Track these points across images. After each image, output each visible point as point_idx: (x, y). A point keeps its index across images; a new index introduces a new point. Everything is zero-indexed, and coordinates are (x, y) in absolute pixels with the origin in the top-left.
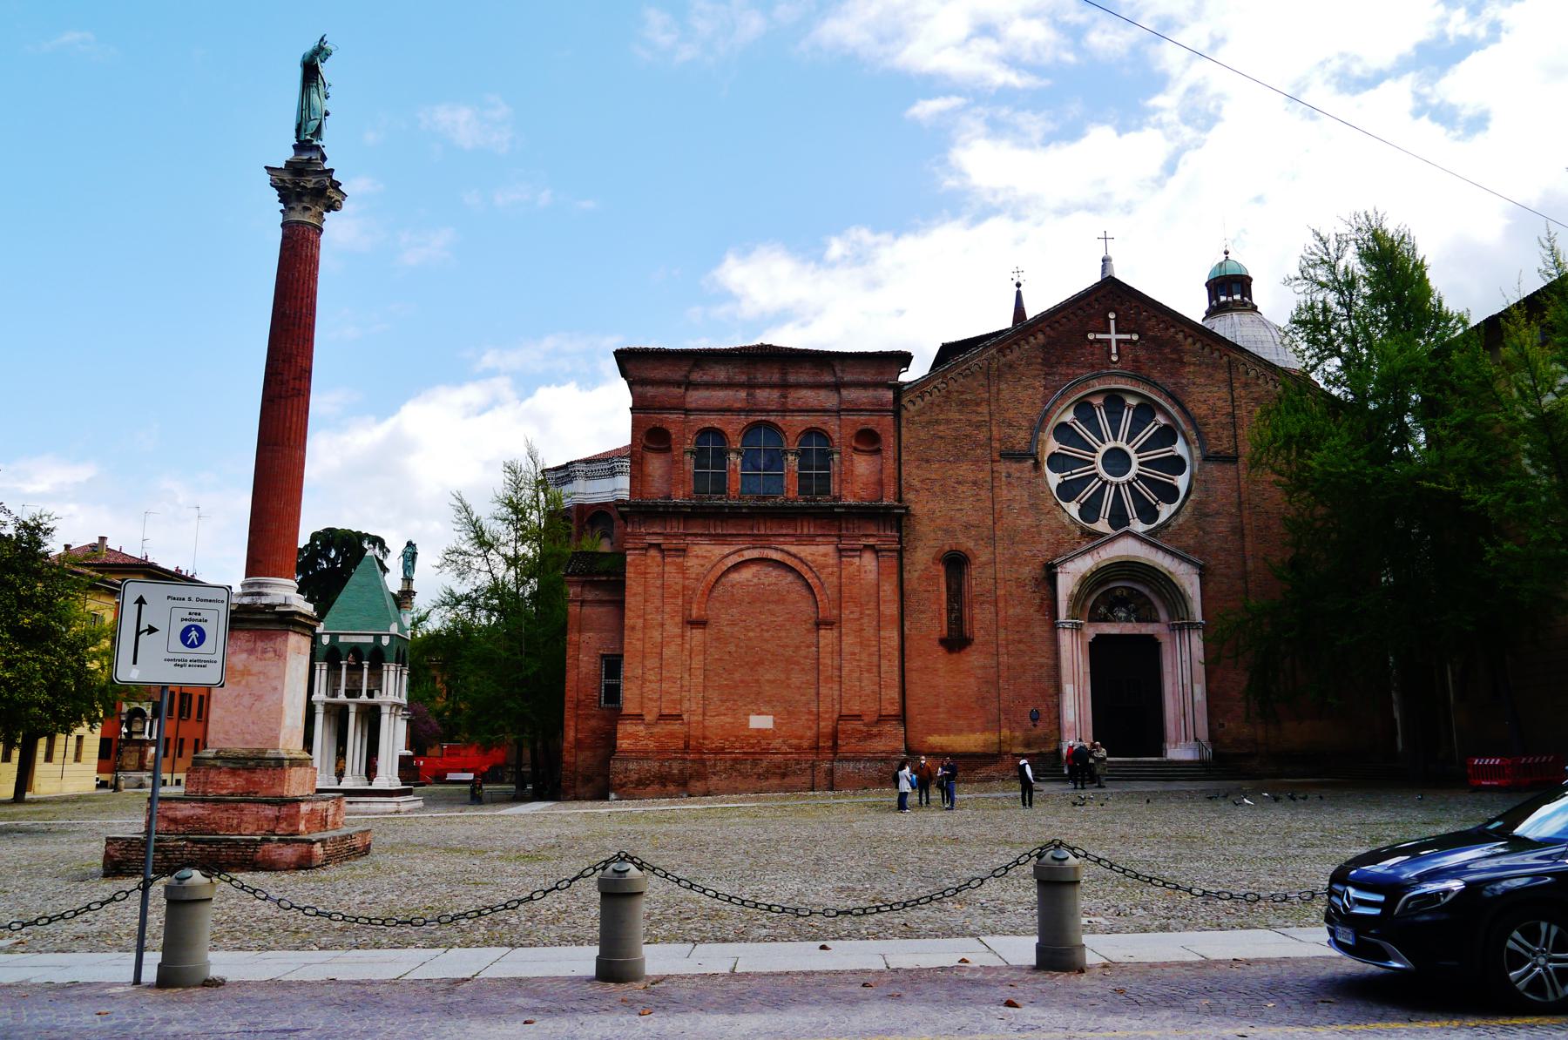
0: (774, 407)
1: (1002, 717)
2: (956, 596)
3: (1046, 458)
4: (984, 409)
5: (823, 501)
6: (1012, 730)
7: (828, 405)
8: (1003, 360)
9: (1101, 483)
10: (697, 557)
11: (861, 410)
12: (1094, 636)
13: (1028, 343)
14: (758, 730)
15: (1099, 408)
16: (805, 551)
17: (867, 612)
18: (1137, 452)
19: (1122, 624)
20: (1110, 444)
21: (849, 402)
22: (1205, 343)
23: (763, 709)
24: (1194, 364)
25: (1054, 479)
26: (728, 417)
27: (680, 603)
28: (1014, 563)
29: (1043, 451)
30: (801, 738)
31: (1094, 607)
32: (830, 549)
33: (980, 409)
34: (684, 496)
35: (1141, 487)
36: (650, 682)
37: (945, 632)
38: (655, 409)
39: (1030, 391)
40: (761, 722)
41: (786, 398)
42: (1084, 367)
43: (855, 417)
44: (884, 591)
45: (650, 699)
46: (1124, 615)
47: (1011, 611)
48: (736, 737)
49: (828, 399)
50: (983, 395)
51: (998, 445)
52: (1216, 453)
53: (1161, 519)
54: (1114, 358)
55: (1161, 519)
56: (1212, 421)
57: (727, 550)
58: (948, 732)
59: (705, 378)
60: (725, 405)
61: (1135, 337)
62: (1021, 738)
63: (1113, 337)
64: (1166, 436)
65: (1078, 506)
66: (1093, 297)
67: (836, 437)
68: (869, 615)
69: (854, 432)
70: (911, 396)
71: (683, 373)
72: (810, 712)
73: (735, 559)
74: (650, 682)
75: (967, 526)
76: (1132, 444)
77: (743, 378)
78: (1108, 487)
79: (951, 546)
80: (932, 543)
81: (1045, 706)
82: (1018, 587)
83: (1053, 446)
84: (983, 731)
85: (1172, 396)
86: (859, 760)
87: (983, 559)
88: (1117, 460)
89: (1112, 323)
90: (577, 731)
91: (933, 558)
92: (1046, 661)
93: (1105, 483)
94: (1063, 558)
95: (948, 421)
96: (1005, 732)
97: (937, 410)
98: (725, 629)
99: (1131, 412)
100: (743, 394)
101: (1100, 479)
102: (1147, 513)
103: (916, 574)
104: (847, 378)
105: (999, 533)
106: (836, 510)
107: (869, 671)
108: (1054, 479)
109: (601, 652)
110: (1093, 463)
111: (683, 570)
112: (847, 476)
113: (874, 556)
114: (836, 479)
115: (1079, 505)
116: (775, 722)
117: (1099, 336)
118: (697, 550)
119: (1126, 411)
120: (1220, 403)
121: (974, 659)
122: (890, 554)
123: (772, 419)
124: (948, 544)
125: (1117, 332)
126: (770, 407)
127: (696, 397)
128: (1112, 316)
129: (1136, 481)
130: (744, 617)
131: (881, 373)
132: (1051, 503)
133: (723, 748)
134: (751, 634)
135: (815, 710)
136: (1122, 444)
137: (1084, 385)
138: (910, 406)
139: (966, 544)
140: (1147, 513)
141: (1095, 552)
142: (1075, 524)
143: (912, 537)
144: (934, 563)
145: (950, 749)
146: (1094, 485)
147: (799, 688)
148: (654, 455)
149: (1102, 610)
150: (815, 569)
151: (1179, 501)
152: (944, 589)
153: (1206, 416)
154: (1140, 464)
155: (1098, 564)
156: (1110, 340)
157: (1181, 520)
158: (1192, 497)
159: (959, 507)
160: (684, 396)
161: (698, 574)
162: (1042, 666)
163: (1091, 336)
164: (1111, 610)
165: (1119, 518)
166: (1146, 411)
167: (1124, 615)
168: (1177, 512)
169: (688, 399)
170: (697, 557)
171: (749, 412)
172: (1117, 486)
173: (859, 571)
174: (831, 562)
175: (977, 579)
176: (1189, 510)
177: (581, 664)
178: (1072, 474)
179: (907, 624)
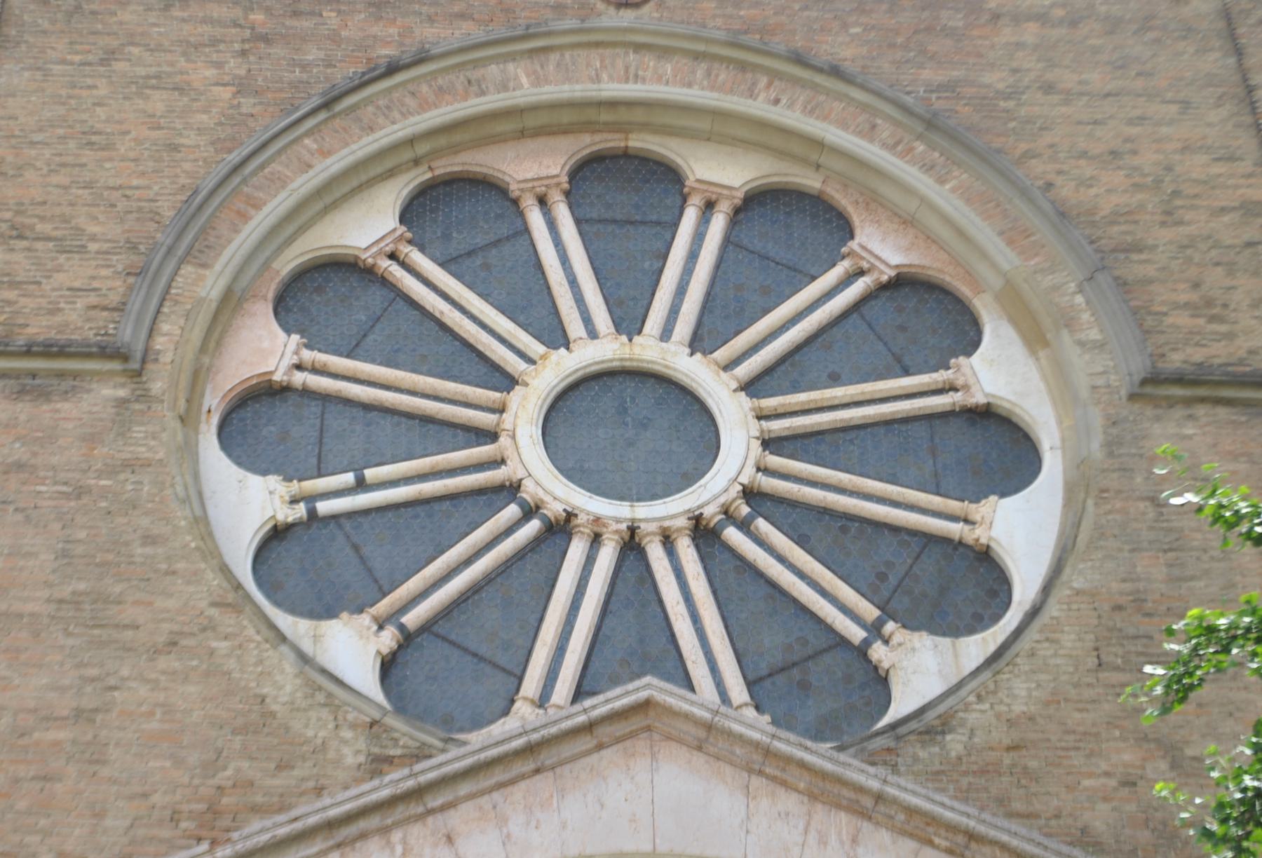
3: (214, 400)
9: (533, 527)
15: (542, 201)
39: (158, 102)
65: (388, 640)
78: (577, 550)
101: (530, 511)
110: (491, 436)
129: (745, 526)
137: (459, 79)
142: (330, 703)
151: (1011, 619)
158: (1077, 578)
172: (632, 546)
176: (1068, 639)
178: (361, 485)
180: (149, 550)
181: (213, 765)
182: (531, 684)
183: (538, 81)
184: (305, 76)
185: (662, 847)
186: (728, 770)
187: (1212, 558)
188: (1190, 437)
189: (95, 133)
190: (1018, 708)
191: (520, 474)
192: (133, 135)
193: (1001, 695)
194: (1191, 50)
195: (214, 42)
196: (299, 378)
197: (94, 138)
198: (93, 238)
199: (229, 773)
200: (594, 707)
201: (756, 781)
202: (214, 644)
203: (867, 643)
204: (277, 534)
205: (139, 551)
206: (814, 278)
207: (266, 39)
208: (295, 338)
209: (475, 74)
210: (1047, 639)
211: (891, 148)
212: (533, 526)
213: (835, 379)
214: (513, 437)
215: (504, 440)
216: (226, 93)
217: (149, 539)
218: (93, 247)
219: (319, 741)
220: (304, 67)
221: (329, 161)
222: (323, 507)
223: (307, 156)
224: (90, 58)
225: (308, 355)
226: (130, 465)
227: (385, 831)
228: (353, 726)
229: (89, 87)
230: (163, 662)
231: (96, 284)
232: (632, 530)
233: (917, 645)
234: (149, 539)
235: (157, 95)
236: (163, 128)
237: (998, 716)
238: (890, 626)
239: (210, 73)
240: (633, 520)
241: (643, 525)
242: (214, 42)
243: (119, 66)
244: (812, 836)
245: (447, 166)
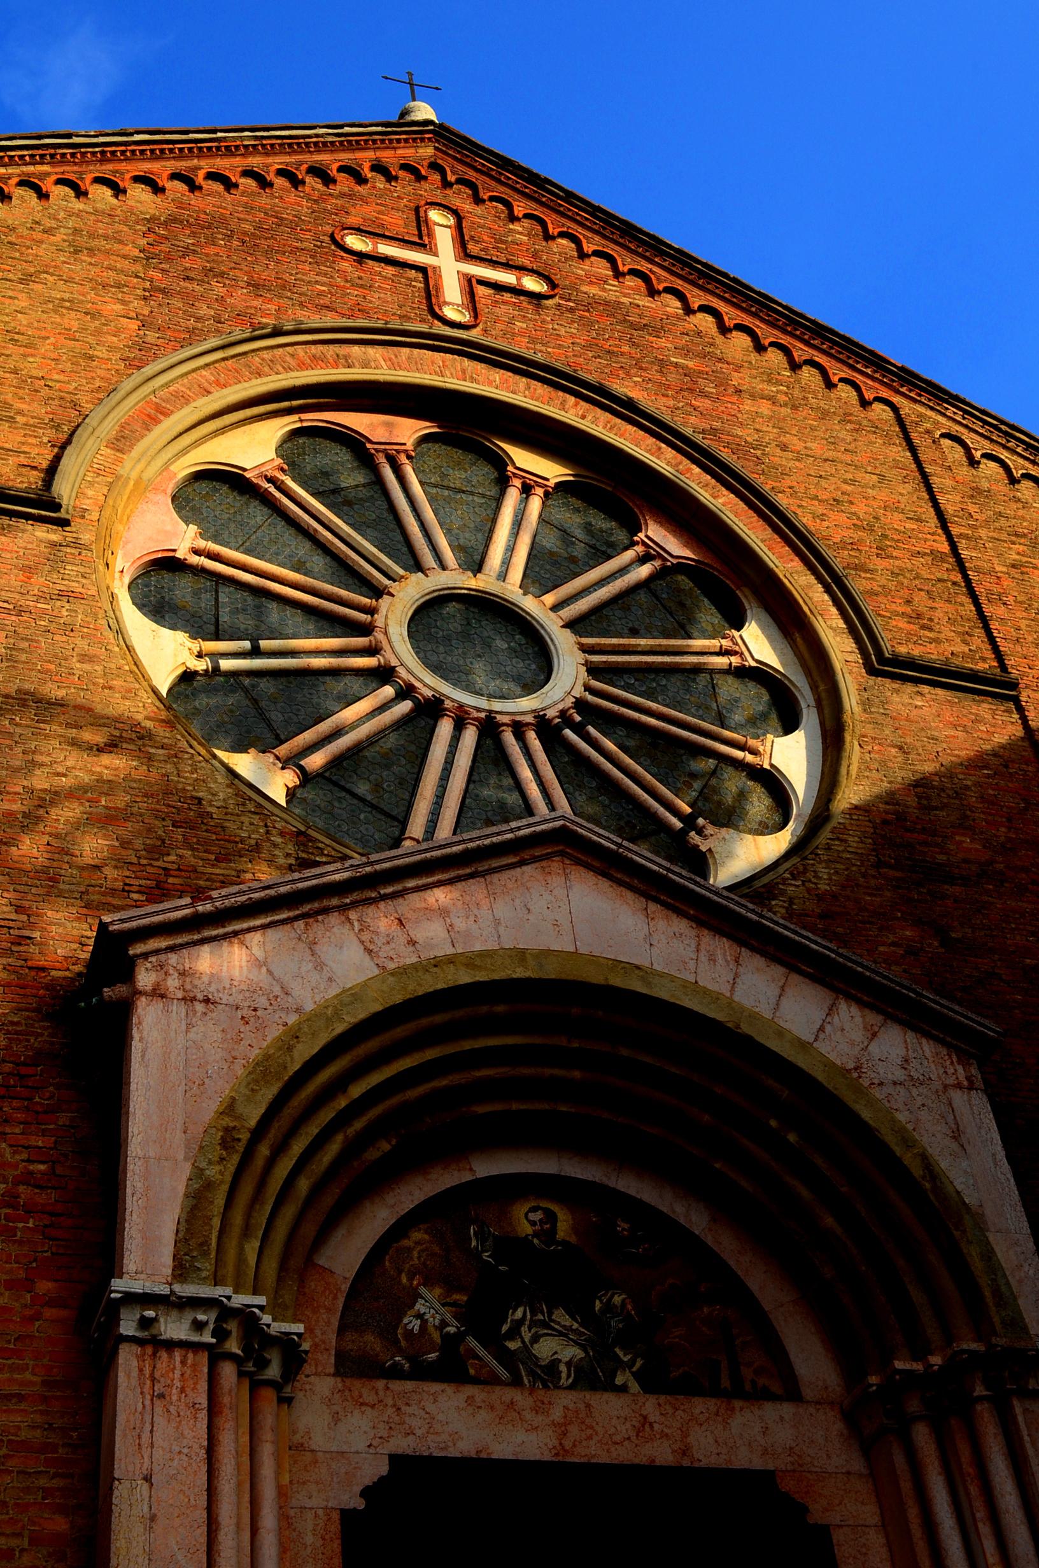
9: (406, 706)
12: (375, 1469)
19: (564, 1401)
24: (772, 399)
39: (72, 321)
46: (571, 1352)
94: (179, 908)
99: (535, 504)
110: (366, 630)
129: (579, 730)
167: (571, 1352)
176: (853, 841)
178: (255, 652)
180: (87, 667)
182: (417, 827)
184: (199, 325)
185: (583, 950)
186: (629, 895)
187: (949, 796)
188: (921, 707)
189: (18, 333)
190: (823, 887)
191: (394, 662)
192: (52, 340)
193: (810, 875)
194: (881, 442)
195: (119, 286)
197: (16, 337)
198: (20, 412)
199: (172, 858)
200: (519, 828)
201: (653, 907)
202: (152, 751)
203: (684, 832)
204: (188, 677)
205: (78, 665)
206: (610, 557)
207: (163, 291)
208: (193, 528)
210: (838, 839)
212: (406, 706)
213: (634, 633)
214: (386, 633)
215: (379, 635)
216: (134, 325)
218: (19, 418)
219: (253, 842)
220: (198, 319)
221: (225, 391)
223: (206, 385)
224: (11, 276)
225: (202, 544)
226: (64, 595)
227: (343, 909)
228: (282, 834)
229: (10, 297)
231: (25, 448)
233: (727, 837)
236: (78, 340)
237: (809, 891)
238: (701, 821)
239: (118, 307)
240: (490, 711)
241: (498, 717)
242: (119, 286)
244: (703, 953)
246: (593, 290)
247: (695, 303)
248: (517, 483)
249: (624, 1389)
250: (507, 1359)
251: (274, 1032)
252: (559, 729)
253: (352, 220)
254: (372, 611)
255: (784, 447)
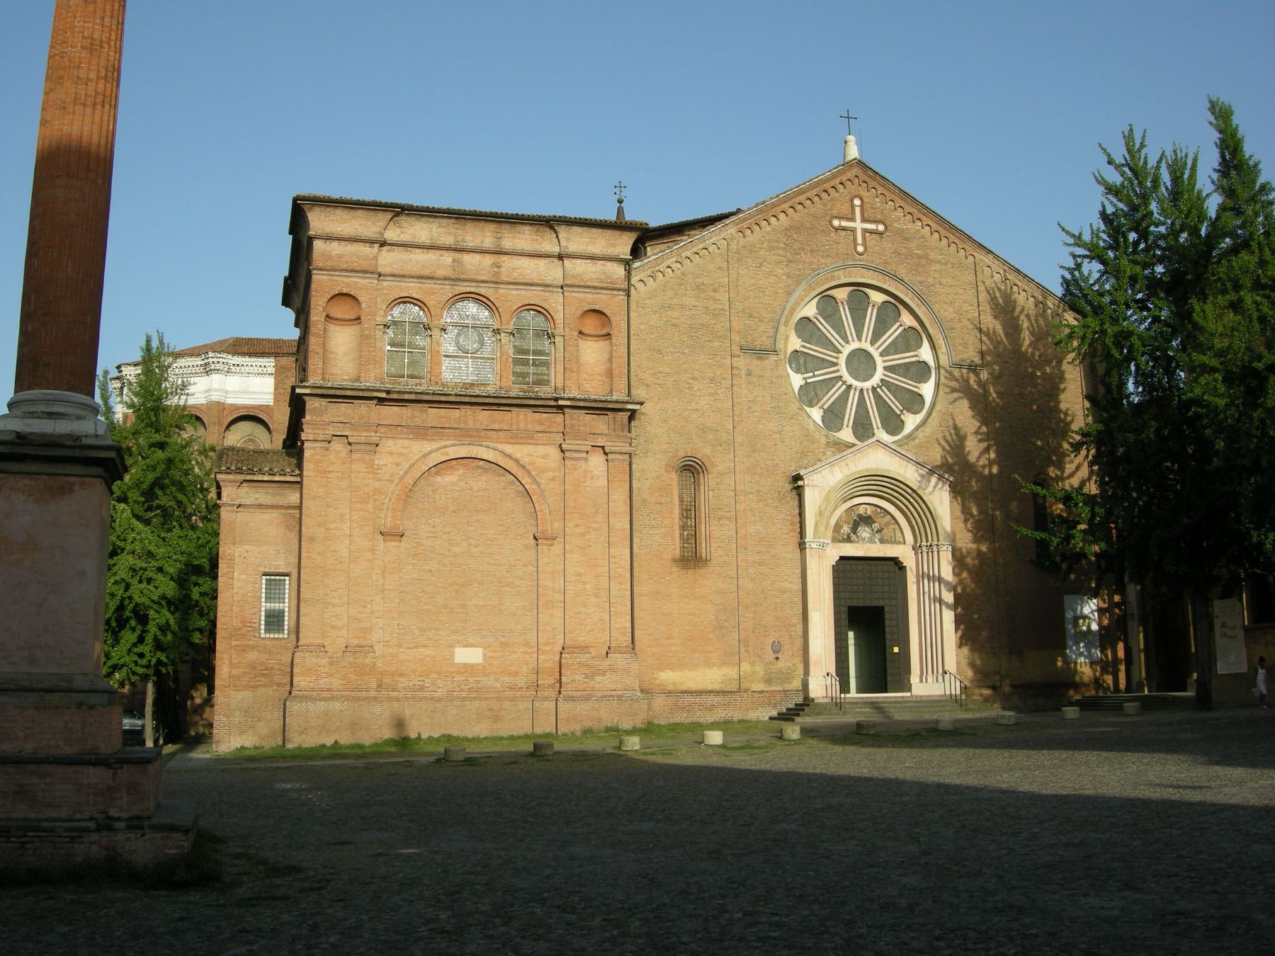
0: (485, 278)
1: (742, 650)
2: (690, 513)
4: (723, 296)
5: (545, 391)
6: (753, 664)
7: (548, 280)
8: (743, 241)
9: (844, 387)
10: (391, 454)
11: (588, 287)
13: (769, 224)
14: (465, 665)
16: (521, 452)
17: (595, 525)
18: (881, 355)
19: (868, 545)
20: (855, 345)
21: (574, 276)
22: (951, 240)
23: (471, 640)
24: (940, 262)
25: (797, 380)
26: (429, 285)
27: (371, 510)
28: (755, 474)
29: (786, 347)
30: (516, 674)
31: (837, 527)
32: (554, 452)
33: (717, 296)
34: (375, 379)
35: (885, 394)
36: (333, 605)
37: (678, 551)
38: (342, 270)
39: (772, 279)
40: (468, 655)
41: (499, 267)
42: (829, 256)
43: (581, 295)
44: (615, 501)
45: (333, 627)
46: (868, 535)
47: (751, 529)
48: (439, 673)
49: (551, 272)
50: (721, 280)
51: (738, 339)
52: (962, 360)
53: (909, 428)
54: (860, 249)
55: (909, 428)
56: (958, 326)
57: (427, 446)
58: (681, 666)
59: (405, 237)
60: (426, 272)
61: (881, 228)
62: (762, 673)
63: (859, 225)
64: (910, 340)
66: (837, 181)
67: (559, 317)
68: (597, 530)
69: (579, 312)
70: (642, 276)
71: (377, 229)
72: (527, 644)
73: (439, 457)
74: (333, 605)
75: (704, 430)
76: (876, 346)
77: (449, 240)
79: (686, 452)
80: (664, 447)
81: (787, 637)
82: (760, 501)
83: (795, 343)
84: (724, 663)
85: (919, 297)
86: (587, 699)
87: (721, 468)
88: (860, 361)
89: (858, 210)
90: (231, 664)
91: (667, 465)
92: (789, 585)
93: (850, 387)
95: (682, 307)
96: (745, 667)
97: (670, 294)
98: (425, 542)
100: (448, 258)
101: (844, 382)
102: (893, 423)
103: (647, 484)
104: (573, 247)
105: (739, 439)
106: (561, 402)
107: (596, 595)
108: (797, 380)
109: (262, 569)
110: (836, 364)
111: (373, 470)
112: (572, 364)
113: (602, 458)
114: (560, 368)
115: (822, 410)
116: (485, 655)
117: (844, 224)
118: (389, 445)
119: (870, 309)
120: (966, 307)
121: (709, 581)
122: (621, 457)
123: (483, 291)
124: (685, 449)
125: (864, 220)
126: (480, 278)
127: (389, 260)
128: (857, 202)
129: (880, 387)
130: (448, 530)
131: (613, 245)
132: (795, 405)
133: (422, 689)
134: (456, 549)
135: (533, 641)
136: (866, 345)
138: (640, 286)
139: (703, 450)
140: (893, 423)
141: (843, 464)
143: (642, 439)
144: (666, 471)
145: (684, 687)
146: (836, 392)
147: (515, 614)
148: (338, 328)
149: (846, 529)
150: (533, 473)
152: (676, 500)
153: (952, 320)
154: (886, 368)
155: (847, 476)
156: (855, 228)
157: (927, 430)
158: (938, 407)
159: (695, 407)
160: (376, 258)
161: (392, 475)
162: (784, 592)
163: (836, 223)
164: (854, 529)
165: (863, 429)
166: (895, 304)
167: (868, 535)
168: (924, 422)
169: (380, 261)
170: (391, 454)
171: (455, 280)
173: (585, 477)
174: (553, 465)
175: (714, 491)
177: (236, 584)
179: (635, 540)
181: (801, 444)
183: (845, 277)
190: (927, 434)
196: (802, 349)
207: (790, 261)
209: (832, 274)
211: (911, 299)
217: (786, 394)
222: (809, 381)
230: (792, 421)
232: (862, 389)
234: (786, 394)
235: (772, 277)
243: (763, 268)
245: (824, 294)
246: (896, 225)
247: (925, 223)
248: (871, 305)
249: (876, 542)
250: (857, 537)
251: (827, 491)
252: (875, 389)
253: (835, 212)
254: (837, 358)
255: (940, 284)
